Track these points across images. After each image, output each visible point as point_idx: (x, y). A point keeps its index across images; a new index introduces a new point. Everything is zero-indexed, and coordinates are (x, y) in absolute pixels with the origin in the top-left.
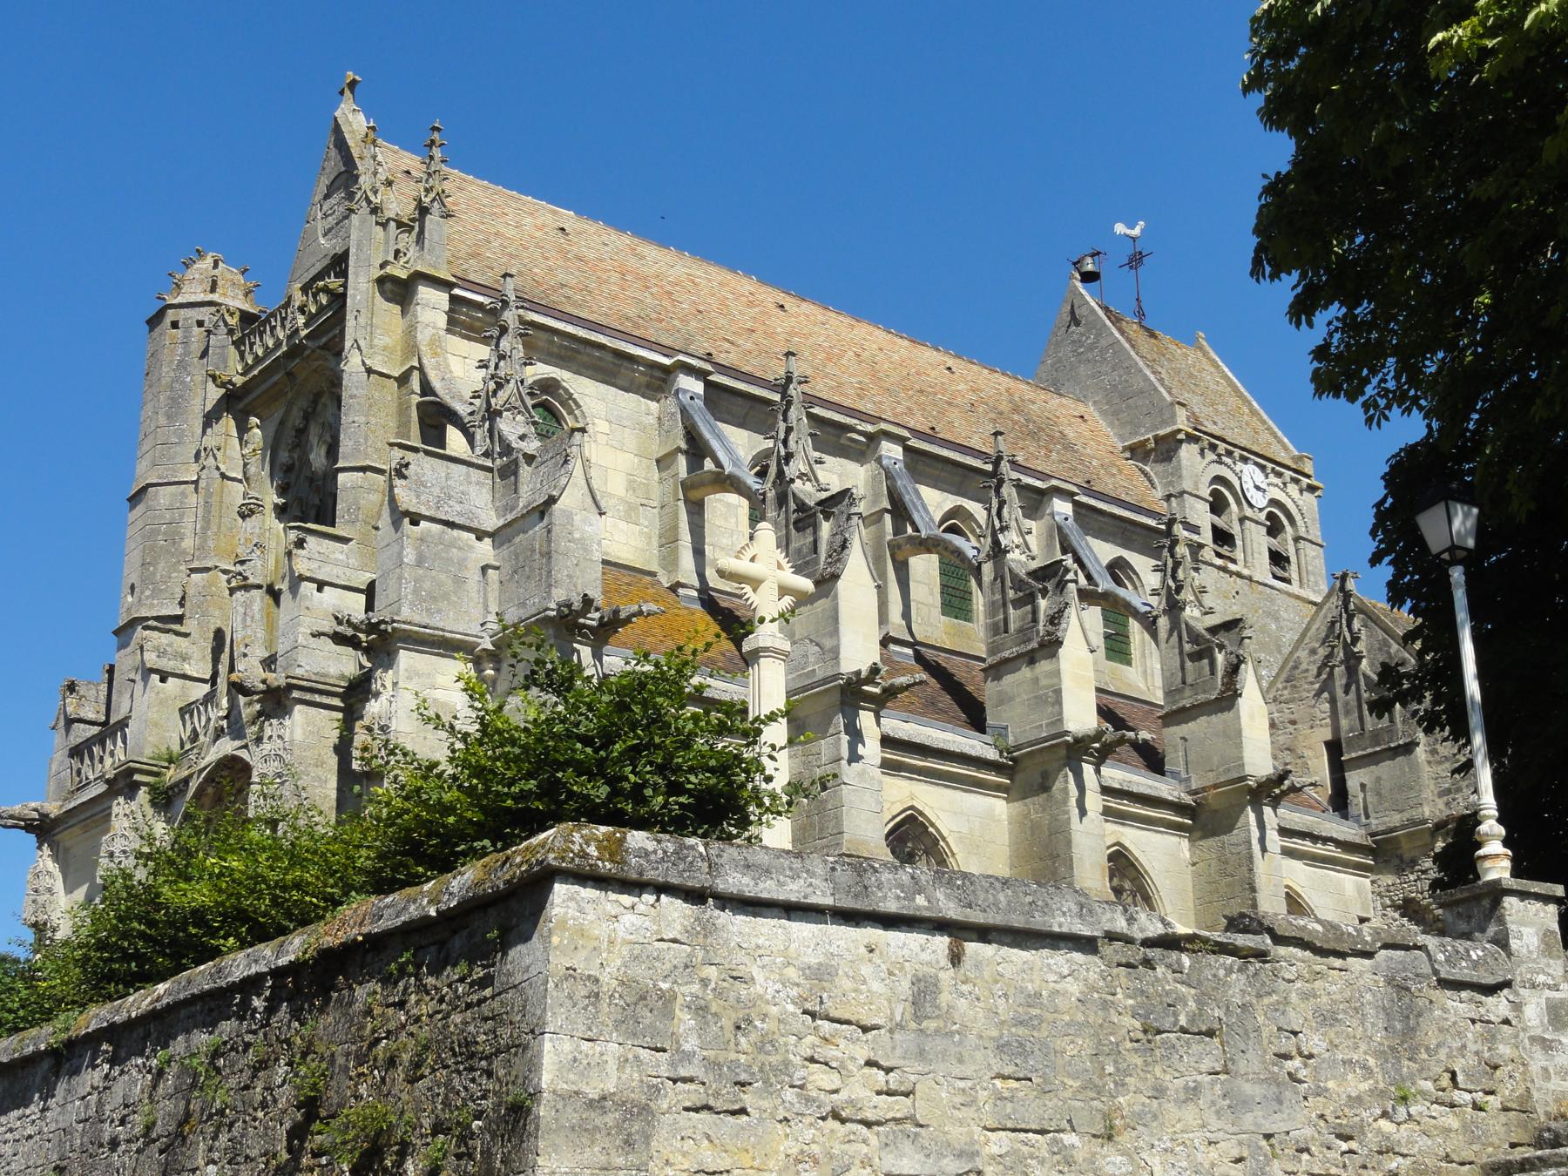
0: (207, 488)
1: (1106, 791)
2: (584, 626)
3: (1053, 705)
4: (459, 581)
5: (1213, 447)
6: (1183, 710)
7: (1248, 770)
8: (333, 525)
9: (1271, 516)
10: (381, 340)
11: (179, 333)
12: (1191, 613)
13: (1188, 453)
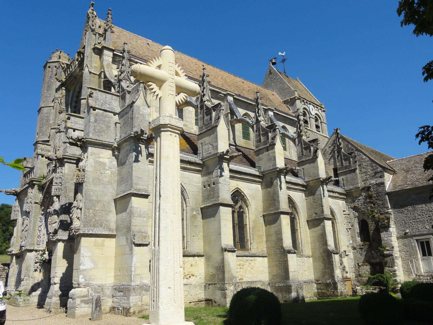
0: (56, 108)
1: (287, 182)
2: (143, 139)
3: (273, 161)
4: (108, 127)
5: (303, 101)
6: (303, 161)
7: (320, 176)
8: (80, 114)
9: (315, 117)
10: (94, 65)
11: (50, 69)
12: (304, 138)
13: (298, 102)
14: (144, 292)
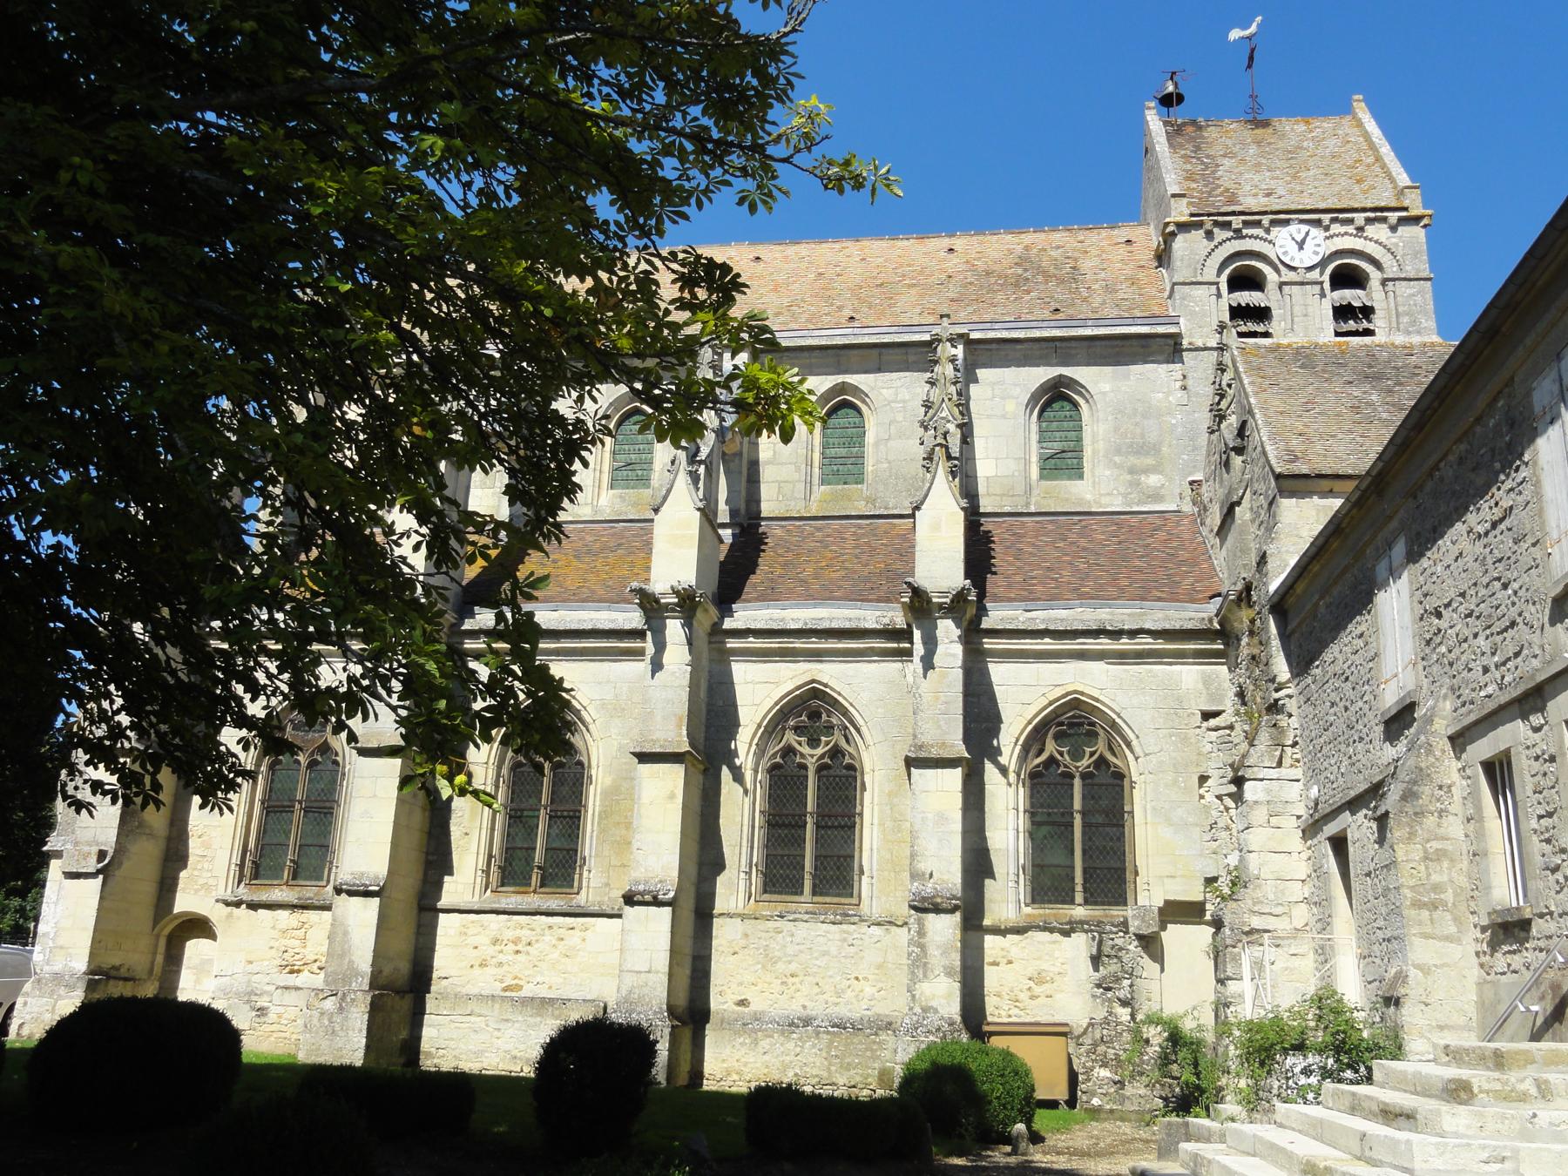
5: (1226, 226)
14: (62, 991)
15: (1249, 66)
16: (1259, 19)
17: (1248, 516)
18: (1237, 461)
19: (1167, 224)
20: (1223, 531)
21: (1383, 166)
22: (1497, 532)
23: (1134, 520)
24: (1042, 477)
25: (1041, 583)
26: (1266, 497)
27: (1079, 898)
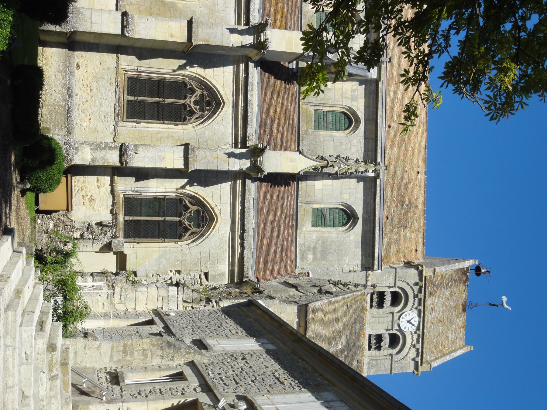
15: (490, 304)
16: (510, 309)
17: (291, 294)
18: (316, 290)
19: (422, 266)
20: (286, 283)
21: (441, 357)
22: (275, 379)
23: (293, 248)
24: (314, 209)
25: (266, 206)
26: (299, 301)
27: (127, 218)
